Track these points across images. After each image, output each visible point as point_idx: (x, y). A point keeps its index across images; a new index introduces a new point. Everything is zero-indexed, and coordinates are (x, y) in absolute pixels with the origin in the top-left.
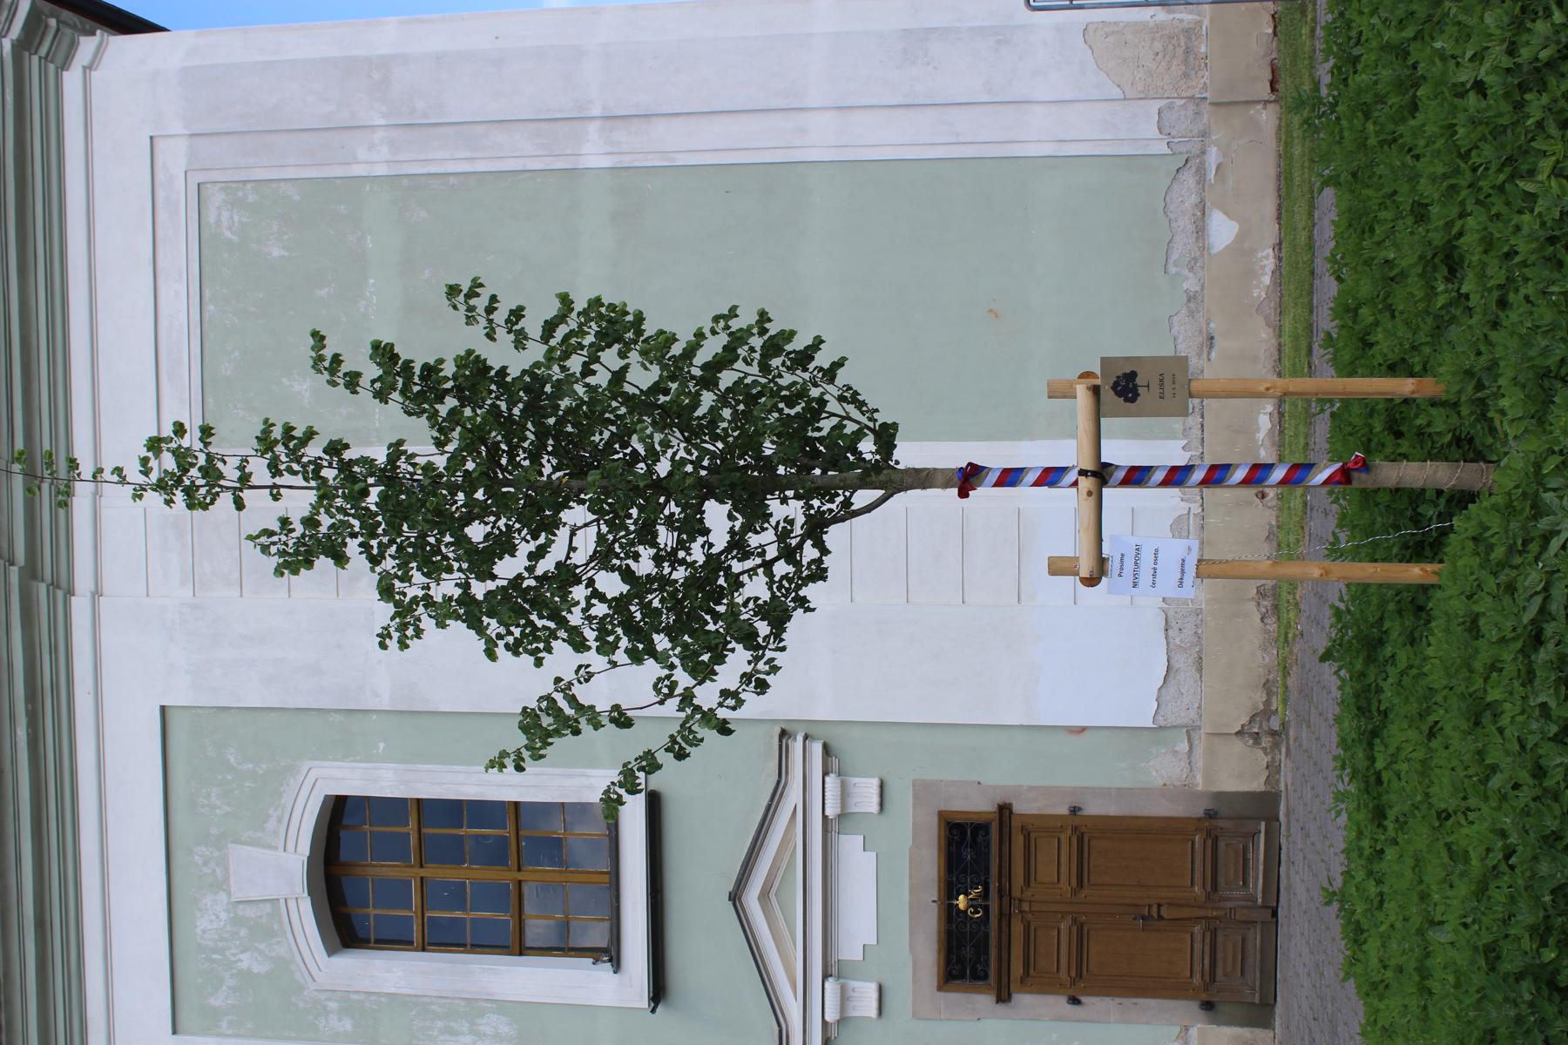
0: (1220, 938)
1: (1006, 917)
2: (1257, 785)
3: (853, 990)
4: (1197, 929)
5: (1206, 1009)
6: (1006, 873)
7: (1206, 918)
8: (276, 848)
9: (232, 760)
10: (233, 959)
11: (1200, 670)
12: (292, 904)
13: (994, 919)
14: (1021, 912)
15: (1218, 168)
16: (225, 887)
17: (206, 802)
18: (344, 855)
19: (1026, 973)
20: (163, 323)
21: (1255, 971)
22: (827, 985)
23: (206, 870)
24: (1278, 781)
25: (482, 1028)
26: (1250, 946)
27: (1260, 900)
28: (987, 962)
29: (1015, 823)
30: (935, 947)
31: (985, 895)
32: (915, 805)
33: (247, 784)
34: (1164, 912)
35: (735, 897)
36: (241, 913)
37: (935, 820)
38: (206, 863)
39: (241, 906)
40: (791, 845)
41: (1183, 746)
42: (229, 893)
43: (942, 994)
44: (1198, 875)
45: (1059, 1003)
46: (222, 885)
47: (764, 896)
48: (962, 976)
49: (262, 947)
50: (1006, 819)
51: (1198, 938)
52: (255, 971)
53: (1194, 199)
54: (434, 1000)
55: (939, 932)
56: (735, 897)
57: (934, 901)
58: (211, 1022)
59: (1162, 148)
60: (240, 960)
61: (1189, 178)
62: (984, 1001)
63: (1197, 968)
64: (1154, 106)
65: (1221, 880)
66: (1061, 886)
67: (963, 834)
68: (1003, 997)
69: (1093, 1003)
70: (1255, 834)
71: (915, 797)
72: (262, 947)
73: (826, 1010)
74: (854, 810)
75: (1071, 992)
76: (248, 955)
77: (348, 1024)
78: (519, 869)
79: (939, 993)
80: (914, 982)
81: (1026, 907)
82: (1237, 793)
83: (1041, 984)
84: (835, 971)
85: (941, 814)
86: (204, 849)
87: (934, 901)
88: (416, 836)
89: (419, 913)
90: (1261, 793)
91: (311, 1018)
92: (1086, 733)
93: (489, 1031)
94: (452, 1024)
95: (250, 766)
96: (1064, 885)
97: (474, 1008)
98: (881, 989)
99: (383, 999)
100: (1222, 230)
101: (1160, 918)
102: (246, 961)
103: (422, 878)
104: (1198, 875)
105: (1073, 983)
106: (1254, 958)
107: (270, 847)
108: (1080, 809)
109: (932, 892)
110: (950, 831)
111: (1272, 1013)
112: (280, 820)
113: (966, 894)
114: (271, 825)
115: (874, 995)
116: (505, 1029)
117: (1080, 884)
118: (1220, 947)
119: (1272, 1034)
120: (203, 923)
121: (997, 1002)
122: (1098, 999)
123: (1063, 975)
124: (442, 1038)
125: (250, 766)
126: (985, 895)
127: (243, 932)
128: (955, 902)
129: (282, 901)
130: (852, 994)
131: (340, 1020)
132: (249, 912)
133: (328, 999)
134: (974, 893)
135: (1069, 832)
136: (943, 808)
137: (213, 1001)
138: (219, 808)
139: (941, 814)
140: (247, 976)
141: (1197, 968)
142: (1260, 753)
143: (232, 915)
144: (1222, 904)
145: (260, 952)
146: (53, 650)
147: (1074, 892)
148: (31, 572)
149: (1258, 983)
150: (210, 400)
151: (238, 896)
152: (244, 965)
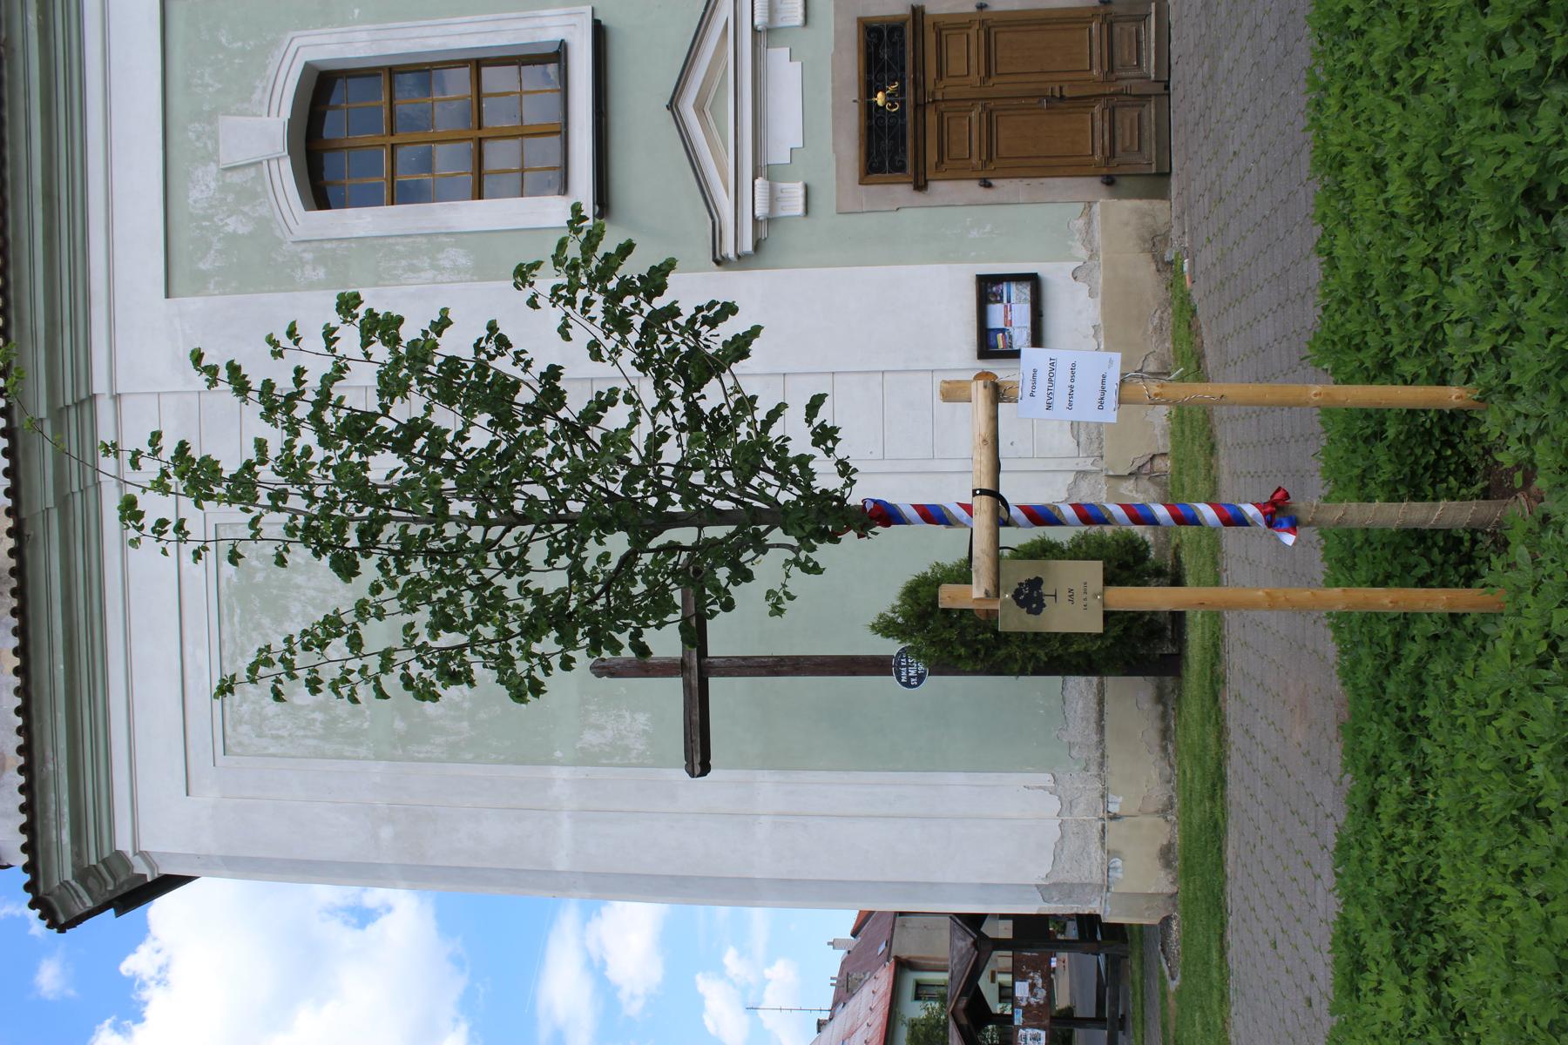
0: (1118, 116)
1: (920, 107)
4: (1097, 109)
6: (920, 67)
7: (1105, 95)
8: (261, 116)
9: (224, 40)
10: (221, 224)
12: (274, 164)
14: (934, 101)
16: (215, 158)
17: (199, 82)
18: (328, 132)
21: (1151, 145)
22: (757, 182)
23: (198, 144)
25: (441, 262)
26: (1145, 122)
27: (1153, 76)
28: (904, 152)
29: (928, 23)
30: (857, 143)
31: (902, 90)
32: (835, 14)
33: (237, 61)
34: (1066, 93)
35: (673, 105)
36: (228, 180)
37: (855, 26)
39: (229, 174)
42: (217, 162)
43: (864, 187)
44: (1096, 59)
45: (972, 188)
46: (212, 156)
47: (699, 108)
49: (246, 209)
50: (919, 18)
51: (1098, 116)
52: (240, 232)
54: (399, 240)
56: (673, 105)
57: (855, 101)
58: (200, 284)
60: (227, 224)
62: (903, 191)
63: (1098, 145)
65: (1117, 62)
66: (971, 77)
67: (880, 38)
68: (920, 186)
69: (1004, 187)
70: (1148, 15)
72: (246, 209)
73: (756, 206)
74: (780, 24)
75: (982, 175)
76: (234, 218)
78: (480, 127)
80: (838, 178)
81: (939, 96)
83: (954, 169)
84: (765, 172)
85: (860, 20)
86: (197, 125)
87: (855, 101)
88: (388, 106)
89: (390, 179)
91: (289, 270)
93: (447, 264)
94: (415, 261)
95: (240, 44)
96: (974, 78)
97: (436, 240)
98: (806, 188)
99: (353, 245)
101: (1062, 97)
102: (234, 225)
103: (393, 145)
104: (1096, 59)
106: (1150, 130)
107: (254, 115)
108: (986, 6)
109: (853, 93)
110: (869, 35)
111: (1168, 185)
113: (884, 90)
114: (257, 96)
115: (800, 192)
116: (462, 261)
118: (1118, 124)
120: (195, 194)
121: (915, 189)
122: (1007, 181)
123: (975, 160)
124: (406, 276)
125: (240, 44)
126: (902, 90)
127: (230, 198)
128: (874, 99)
129: (265, 163)
130: (782, 195)
131: (314, 270)
132: (235, 178)
133: (304, 251)
134: (891, 89)
135: (977, 27)
136: (861, 14)
137: (202, 266)
138: (212, 86)
139: (860, 20)
140: (233, 238)
141: (1098, 145)
143: (221, 183)
144: (1118, 82)
145: (245, 214)
147: (983, 81)
149: (1154, 153)
151: (226, 161)
152: (230, 229)
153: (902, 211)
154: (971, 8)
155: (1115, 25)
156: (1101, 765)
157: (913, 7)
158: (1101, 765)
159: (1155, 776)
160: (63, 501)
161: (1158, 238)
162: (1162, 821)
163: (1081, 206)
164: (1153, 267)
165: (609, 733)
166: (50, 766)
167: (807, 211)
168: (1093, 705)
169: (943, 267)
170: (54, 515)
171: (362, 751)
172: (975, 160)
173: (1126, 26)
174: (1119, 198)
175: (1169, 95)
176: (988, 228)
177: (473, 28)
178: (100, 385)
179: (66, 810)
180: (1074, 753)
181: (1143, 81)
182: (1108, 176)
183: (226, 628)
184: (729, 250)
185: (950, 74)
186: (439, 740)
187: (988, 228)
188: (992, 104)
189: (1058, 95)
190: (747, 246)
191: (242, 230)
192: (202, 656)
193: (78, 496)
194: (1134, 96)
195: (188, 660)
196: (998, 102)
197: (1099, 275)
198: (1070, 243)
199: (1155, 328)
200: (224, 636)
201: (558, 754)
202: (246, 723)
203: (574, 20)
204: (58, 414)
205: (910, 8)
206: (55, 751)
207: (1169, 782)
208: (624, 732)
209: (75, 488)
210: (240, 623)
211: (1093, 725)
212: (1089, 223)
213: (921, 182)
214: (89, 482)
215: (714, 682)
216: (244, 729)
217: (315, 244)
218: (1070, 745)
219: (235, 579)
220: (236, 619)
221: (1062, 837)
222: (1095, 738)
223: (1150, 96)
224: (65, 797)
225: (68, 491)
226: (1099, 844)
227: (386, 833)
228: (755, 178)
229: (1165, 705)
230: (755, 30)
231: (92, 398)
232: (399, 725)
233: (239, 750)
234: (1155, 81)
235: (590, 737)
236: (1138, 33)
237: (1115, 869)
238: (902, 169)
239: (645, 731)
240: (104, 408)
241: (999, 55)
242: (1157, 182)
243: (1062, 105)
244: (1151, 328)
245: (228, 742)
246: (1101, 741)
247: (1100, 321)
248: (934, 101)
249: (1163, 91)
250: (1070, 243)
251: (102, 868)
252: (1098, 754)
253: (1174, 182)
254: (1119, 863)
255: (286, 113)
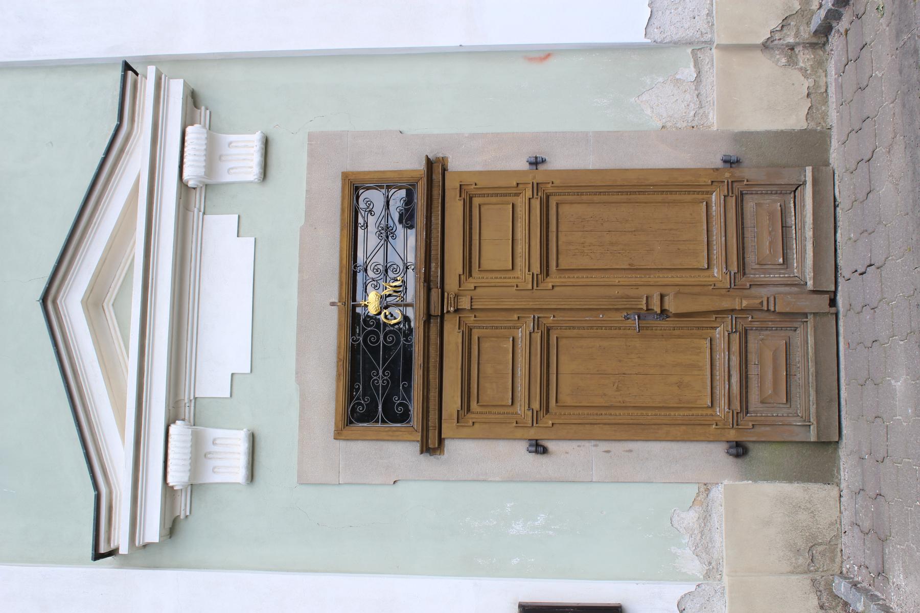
0: (753, 345)
2: (796, 121)
3: (214, 443)
4: (720, 333)
5: (737, 456)
7: (733, 311)
19: (466, 406)
22: (173, 429)
24: (825, 115)
26: (797, 356)
27: (810, 283)
28: (408, 390)
29: (452, 184)
32: (310, 166)
34: (671, 305)
37: (338, 184)
41: (689, 73)
43: (342, 444)
48: (368, 416)
50: (437, 177)
55: (339, 347)
57: (333, 304)
63: (721, 391)
65: (751, 258)
66: (518, 273)
71: (311, 154)
73: (169, 469)
75: (533, 433)
79: (337, 442)
81: (465, 303)
82: (767, 133)
84: (188, 412)
87: (333, 304)
90: (803, 132)
92: (553, 62)
96: (523, 276)
98: (253, 440)
105: (536, 419)
106: (806, 370)
108: (543, 161)
111: (834, 461)
117: (545, 269)
118: (753, 358)
119: (835, 492)
121: (422, 452)
122: (574, 444)
123: (521, 407)
135: (529, 193)
136: (349, 168)
141: (721, 391)
142: (796, 76)
144: (754, 291)
147: (536, 281)
149: (813, 409)
153: (398, 483)
154: (522, 165)
155: (746, 197)
157: (428, 159)
161: (820, 548)
163: (692, 490)
164: (815, 602)
167: (252, 476)
169: (466, 585)
172: (521, 407)
173: (767, 201)
174: (755, 481)
175: (837, 315)
176: (541, 519)
181: (795, 289)
182: (738, 444)
184: (121, 539)
185: (486, 265)
187: (541, 519)
188: (550, 320)
189: (658, 309)
190: (152, 531)
194: (780, 313)
196: (560, 316)
198: (674, 549)
205: (424, 162)
212: (706, 517)
213: (433, 442)
223: (805, 315)
230: (184, 188)
234: (814, 292)
238: (404, 417)
241: (562, 238)
243: (664, 324)
248: (457, 311)
249: (825, 307)
250: (674, 549)
253: (843, 452)
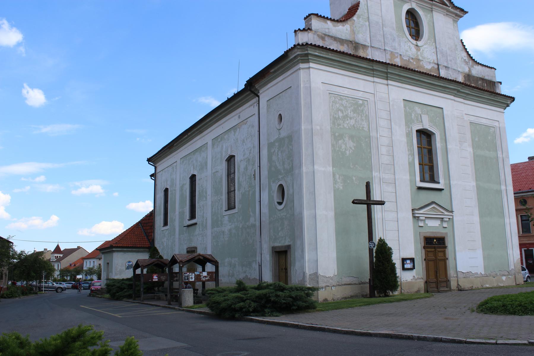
0: (434, 283)
1: (434, 248)
2: (452, 288)
11: (464, 278)
12: (422, 125)
13: (434, 246)
15: (509, 277)
20: (482, 118)
29: (444, 249)
31: (436, 244)
37: (443, 236)
38: (424, 111)
40: (437, 212)
45: (424, 257)
47: (434, 208)
53: (506, 274)
56: (433, 203)
59: (510, 270)
61: (507, 273)
62: (423, 244)
64: (514, 268)
69: (424, 262)
70: (447, 288)
72: (415, 118)
77: (407, 132)
85: (445, 237)
92: (454, 260)
93: (410, 157)
97: (413, 155)
100: (504, 278)
112: (431, 125)
113: (436, 241)
114: (431, 123)
120: (417, 108)
127: (417, 115)
129: (422, 123)
136: (446, 237)
146: (449, 92)
148: (458, 91)
150: (474, 124)
151: (422, 115)
156: (338, 285)
158: (338, 285)
159: (339, 296)
160: (373, 70)
162: (332, 298)
164: (416, 291)
165: (338, 180)
166: (330, 54)
168: (349, 283)
169: (414, 252)
170: (372, 68)
171: (332, 125)
173: (445, 285)
176: (419, 260)
177: (441, 166)
178: (390, 82)
179: (322, 55)
180: (340, 279)
183: (351, 99)
186: (335, 143)
187: (419, 260)
190: (417, 215)
191: (412, 116)
192: (346, 92)
193: (373, 73)
195: (345, 89)
197: (413, 281)
199: (408, 291)
200: (349, 98)
201: (334, 169)
202: (335, 99)
203: (443, 185)
204: (387, 73)
206: (332, 56)
207: (337, 300)
208: (339, 184)
209: (374, 73)
210: (352, 102)
211: (345, 283)
212: (420, 279)
213: (425, 248)
214: (374, 76)
215: (366, 206)
216: (334, 99)
217: (411, 131)
218: (341, 278)
219: (359, 103)
220: (352, 101)
221: (327, 277)
222: (343, 283)
223: (438, 289)
224: (324, 56)
225: (374, 71)
226: (326, 285)
227: (318, 128)
228: (425, 217)
229: (350, 298)
230: (442, 218)
231: (387, 80)
232: (337, 134)
233: (330, 96)
235: (337, 176)
236: (445, 287)
237: (323, 289)
238: (426, 244)
239: (339, 188)
240: (385, 82)
242: (427, 291)
244: (408, 291)
245: (331, 94)
246: (343, 285)
247: (408, 281)
251: (307, 58)
252: (340, 284)
254: (324, 290)
255: (429, 129)
